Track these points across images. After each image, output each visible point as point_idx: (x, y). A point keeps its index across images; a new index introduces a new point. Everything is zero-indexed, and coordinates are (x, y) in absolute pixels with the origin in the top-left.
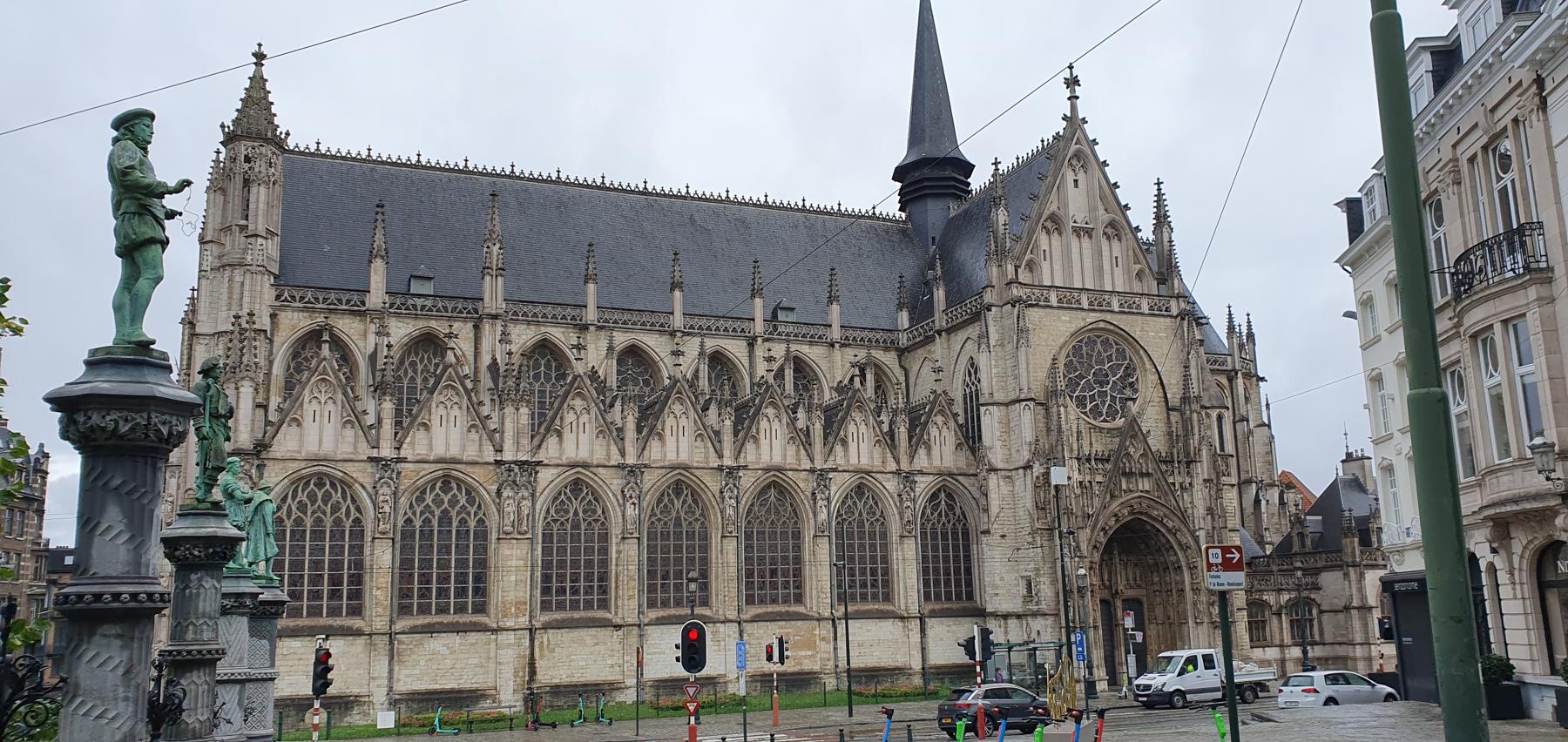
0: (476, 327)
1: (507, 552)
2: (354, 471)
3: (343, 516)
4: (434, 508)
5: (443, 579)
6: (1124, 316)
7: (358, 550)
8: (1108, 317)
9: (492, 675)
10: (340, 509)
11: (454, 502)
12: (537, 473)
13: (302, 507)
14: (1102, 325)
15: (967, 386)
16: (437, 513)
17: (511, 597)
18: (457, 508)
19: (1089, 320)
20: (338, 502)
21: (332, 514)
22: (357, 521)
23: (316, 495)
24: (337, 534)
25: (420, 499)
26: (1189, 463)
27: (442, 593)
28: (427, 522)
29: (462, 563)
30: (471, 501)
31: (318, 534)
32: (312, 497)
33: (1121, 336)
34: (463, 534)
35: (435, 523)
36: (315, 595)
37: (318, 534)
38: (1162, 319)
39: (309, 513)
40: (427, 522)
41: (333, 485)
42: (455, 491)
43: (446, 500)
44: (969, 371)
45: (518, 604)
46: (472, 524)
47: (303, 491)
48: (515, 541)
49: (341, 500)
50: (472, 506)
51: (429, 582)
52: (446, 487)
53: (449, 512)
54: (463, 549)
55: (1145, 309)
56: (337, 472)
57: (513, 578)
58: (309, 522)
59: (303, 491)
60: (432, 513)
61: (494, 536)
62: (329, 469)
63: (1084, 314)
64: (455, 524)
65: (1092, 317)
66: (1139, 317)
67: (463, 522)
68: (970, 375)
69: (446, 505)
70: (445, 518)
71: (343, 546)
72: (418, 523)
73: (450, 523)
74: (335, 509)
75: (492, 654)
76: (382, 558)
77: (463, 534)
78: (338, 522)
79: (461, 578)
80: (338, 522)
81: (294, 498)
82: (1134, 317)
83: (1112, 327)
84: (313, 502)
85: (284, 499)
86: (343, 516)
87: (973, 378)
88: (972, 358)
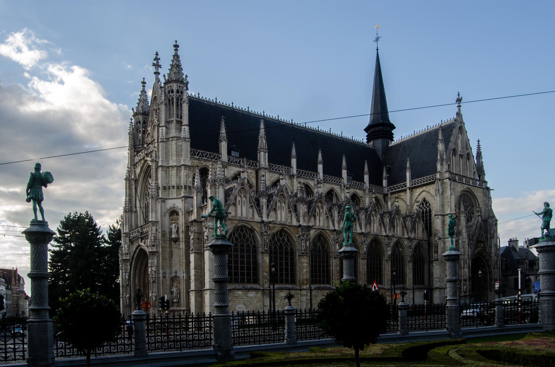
0: (257, 173)
1: (303, 260)
4: (278, 242)
6: (473, 187)
7: (255, 257)
8: (469, 187)
9: (299, 306)
11: (283, 240)
12: (310, 230)
13: (237, 239)
14: (468, 190)
16: (279, 244)
17: (305, 277)
18: (285, 243)
20: (248, 238)
21: (246, 243)
22: (254, 246)
23: (241, 235)
24: (248, 251)
28: (275, 248)
29: (287, 264)
30: (288, 240)
32: (240, 235)
33: (471, 194)
35: (278, 248)
36: (242, 274)
37: (242, 251)
38: (481, 189)
39: (239, 242)
40: (275, 248)
41: (246, 231)
42: (284, 236)
43: (281, 239)
44: (422, 203)
45: (307, 280)
46: (289, 249)
48: (305, 257)
49: (249, 237)
50: (289, 242)
52: (281, 235)
53: (282, 244)
54: (287, 259)
56: (249, 226)
57: (305, 270)
58: (239, 245)
59: (237, 233)
60: (277, 244)
61: (297, 254)
62: (246, 224)
64: (284, 248)
67: (286, 249)
68: (423, 204)
70: (281, 247)
72: (273, 247)
73: (283, 249)
74: (247, 241)
75: (299, 298)
76: (264, 260)
77: (286, 253)
78: (248, 246)
79: (287, 270)
80: (248, 246)
81: (234, 236)
83: (470, 191)
84: (240, 237)
88: (424, 198)
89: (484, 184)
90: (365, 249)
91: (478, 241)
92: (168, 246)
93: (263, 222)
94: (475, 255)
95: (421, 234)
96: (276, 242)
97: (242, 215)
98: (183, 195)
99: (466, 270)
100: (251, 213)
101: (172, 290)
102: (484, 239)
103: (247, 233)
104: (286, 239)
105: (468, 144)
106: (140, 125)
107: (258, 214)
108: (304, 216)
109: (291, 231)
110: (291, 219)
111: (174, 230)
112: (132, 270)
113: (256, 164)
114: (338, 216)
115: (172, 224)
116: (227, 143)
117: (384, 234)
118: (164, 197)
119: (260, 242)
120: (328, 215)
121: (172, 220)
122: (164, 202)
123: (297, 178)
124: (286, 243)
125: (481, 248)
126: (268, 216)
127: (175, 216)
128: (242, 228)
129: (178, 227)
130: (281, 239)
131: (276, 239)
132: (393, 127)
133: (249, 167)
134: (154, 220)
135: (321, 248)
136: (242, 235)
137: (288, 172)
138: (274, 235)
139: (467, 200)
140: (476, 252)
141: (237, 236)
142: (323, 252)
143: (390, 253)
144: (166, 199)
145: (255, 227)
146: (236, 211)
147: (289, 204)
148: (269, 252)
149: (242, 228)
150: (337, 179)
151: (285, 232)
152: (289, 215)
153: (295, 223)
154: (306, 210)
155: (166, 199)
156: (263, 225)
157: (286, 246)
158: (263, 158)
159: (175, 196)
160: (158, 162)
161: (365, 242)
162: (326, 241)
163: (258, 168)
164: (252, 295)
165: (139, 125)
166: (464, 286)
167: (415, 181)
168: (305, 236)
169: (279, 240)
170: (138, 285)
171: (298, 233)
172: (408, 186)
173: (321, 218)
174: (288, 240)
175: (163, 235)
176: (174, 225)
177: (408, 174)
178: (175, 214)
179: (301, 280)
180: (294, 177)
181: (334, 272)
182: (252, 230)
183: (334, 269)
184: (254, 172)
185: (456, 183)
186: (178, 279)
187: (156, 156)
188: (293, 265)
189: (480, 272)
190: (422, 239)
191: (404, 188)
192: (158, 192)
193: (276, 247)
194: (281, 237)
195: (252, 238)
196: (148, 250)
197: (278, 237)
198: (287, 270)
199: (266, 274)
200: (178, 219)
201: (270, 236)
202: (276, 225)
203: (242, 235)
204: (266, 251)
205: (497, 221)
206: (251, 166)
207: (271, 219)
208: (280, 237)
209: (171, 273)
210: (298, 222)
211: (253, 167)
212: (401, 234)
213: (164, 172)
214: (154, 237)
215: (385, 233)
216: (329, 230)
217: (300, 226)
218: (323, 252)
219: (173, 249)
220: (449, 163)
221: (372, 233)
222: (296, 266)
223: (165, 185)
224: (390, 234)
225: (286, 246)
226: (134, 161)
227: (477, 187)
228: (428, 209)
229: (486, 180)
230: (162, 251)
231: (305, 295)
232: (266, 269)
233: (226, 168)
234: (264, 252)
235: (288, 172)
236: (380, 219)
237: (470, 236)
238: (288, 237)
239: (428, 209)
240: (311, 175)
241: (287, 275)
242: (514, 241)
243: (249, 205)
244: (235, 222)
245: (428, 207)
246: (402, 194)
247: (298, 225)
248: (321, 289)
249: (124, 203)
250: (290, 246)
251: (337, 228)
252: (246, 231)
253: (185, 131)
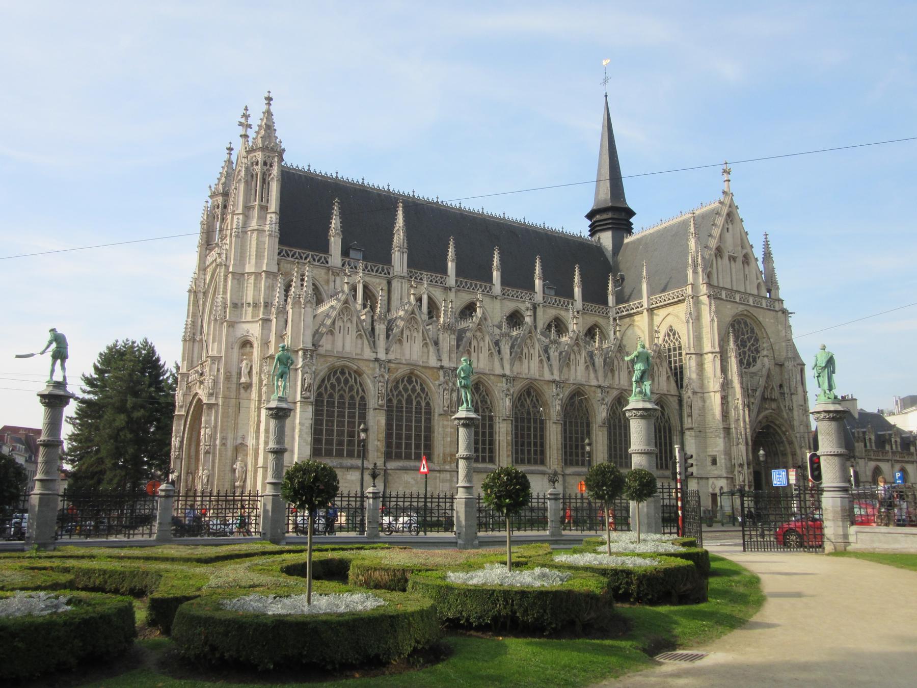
2: (364, 367)
3: (355, 394)
4: (403, 393)
5: (409, 437)
8: (748, 308)
10: (353, 389)
11: (414, 390)
13: (333, 386)
14: (745, 313)
15: (667, 342)
16: (405, 396)
18: (416, 394)
19: (740, 309)
20: (352, 385)
22: (363, 398)
24: (352, 406)
25: (396, 387)
26: (791, 394)
27: (408, 446)
28: (400, 401)
29: (418, 428)
31: (341, 405)
32: (338, 380)
33: (753, 319)
34: (418, 412)
35: (404, 403)
36: (340, 443)
37: (341, 405)
38: (772, 312)
39: (337, 390)
40: (400, 401)
41: (350, 374)
43: (410, 388)
46: (423, 404)
47: (334, 376)
50: (423, 393)
51: (401, 439)
54: (418, 421)
55: (764, 305)
57: (449, 439)
58: (336, 396)
59: (334, 376)
60: (402, 396)
63: (737, 305)
64: (414, 403)
65: (741, 308)
66: (762, 310)
67: (418, 403)
68: (669, 335)
69: (410, 392)
70: (409, 401)
71: (355, 413)
72: (395, 402)
74: (351, 389)
76: (377, 421)
77: (418, 412)
78: (352, 397)
79: (418, 437)
80: (352, 397)
81: (329, 381)
82: (759, 309)
85: (323, 381)
86: (355, 394)
87: (672, 338)
88: (671, 326)
89: (776, 303)
90: (558, 408)
91: (764, 399)
92: (233, 395)
93: (377, 360)
94: (760, 422)
95: (665, 384)
96: (400, 392)
97: (343, 349)
98: (261, 317)
99: (742, 447)
100: (360, 346)
101: (234, 466)
102: (776, 394)
103: (351, 377)
104: (418, 388)
105: (745, 238)
106: (219, 212)
107: (371, 348)
108: (450, 351)
109: (426, 376)
110: (428, 356)
111: (244, 371)
112: (186, 432)
113: (387, 270)
114: (511, 353)
115: (242, 361)
116: (342, 239)
117: (594, 382)
118: (233, 319)
119: (372, 392)
120: (493, 351)
121: (243, 355)
122: (233, 327)
123: (456, 292)
124: (419, 394)
125: (771, 411)
126: (387, 351)
127: (248, 349)
128: (343, 370)
129: (251, 367)
130: (410, 388)
131: (401, 387)
132: (631, 213)
133: (377, 274)
134: (215, 353)
135: (479, 403)
136: (342, 380)
137: (441, 283)
138: (397, 382)
139: (745, 330)
140: (761, 417)
141: (334, 381)
142: (484, 410)
143: (604, 414)
144: (237, 323)
145: (364, 368)
146: (333, 343)
147: (425, 333)
148: (385, 408)
149: (343, 370)
150: (526, 294)
151: (417, 376)
152: (426, 350)
153: (433, 362)
154: (454, 343)
155: (237, 323)
156: (377, 365)
157: (419, 399)
158: (399, 260)
159: (249, 318)
160: (229, 266)
161: (558, 395)
162: (488, 392)
163: (391, 275)
164: (353, 478)
165: (216, 210)
166: (739, 476)
167: (656, 298)
168: (451, 384)
169: (406, 389)
170: (193, 457)
171: (438, 379)
172: (645, 306)
173: (481, 356)
174: (423, 390)
175: (228, 378)
176: (245, 362)
177: (644, 287)
178: (248, 346)
179: (441, 455)
180: (450, 290)
181: (501, 443)
182: (359, 373)
183: (501, 438)
184: (385, 282)
185: (721, 301)
186: (245, 448)
187: (226, 258)
188: (429, 430)
189: (762, 452)
190: (666, 393)
191: (640, 309)
192: (225, 312)
193: (401, 401)
194: (410, 384)
195: (358, 385)
196: (205, 401)
197: (405, 385)
198: (418, 437)
199: (379, 443)
200: (252, 352)
201: (390, 381)
202: (402, 366)
203: (342, 380)
204: (381, 406)
205: (804, 365)
206: (380, 273)
207: (391, 356)
208: (408, 385)
209: (235, 439)
210: (439, 362)
211: (383, 275)
212: (626, 384)
213: (236, 282)
214: (214, 380)
215: (595, 381)
216: (494, 375)
217: (442, 367)
218: (484, 410)
219: (241, 401)
220: (709, 269)
221: (571, 381)
222: (434, 432)
223: (236, 301)
224: (606, 384)
225: (419, 399)
226: (205, 263)
227: (763, 308)
228: (677, 343)
229: (781, 297)
230: (223, 402)
231: (447, 480)
232: (380, 435)
233: (338, 275)
234: (377, 407)
235: (441, 283)
236: (588, 359)
237: (748, 389)
238: (421, 385)
239: (677, 343)
240: (471, 286)
241: (418, 447)
242: (848, 400)
243: (355, 334)
244: (331, 359)
245: (677, 340)
246: (636, 318)
247: (438, 365)
248: (478, 472)
249: (184, 330)
250: (425, 399)
251: (508, 372)
252: (350, 374)
253: (272, 218)
